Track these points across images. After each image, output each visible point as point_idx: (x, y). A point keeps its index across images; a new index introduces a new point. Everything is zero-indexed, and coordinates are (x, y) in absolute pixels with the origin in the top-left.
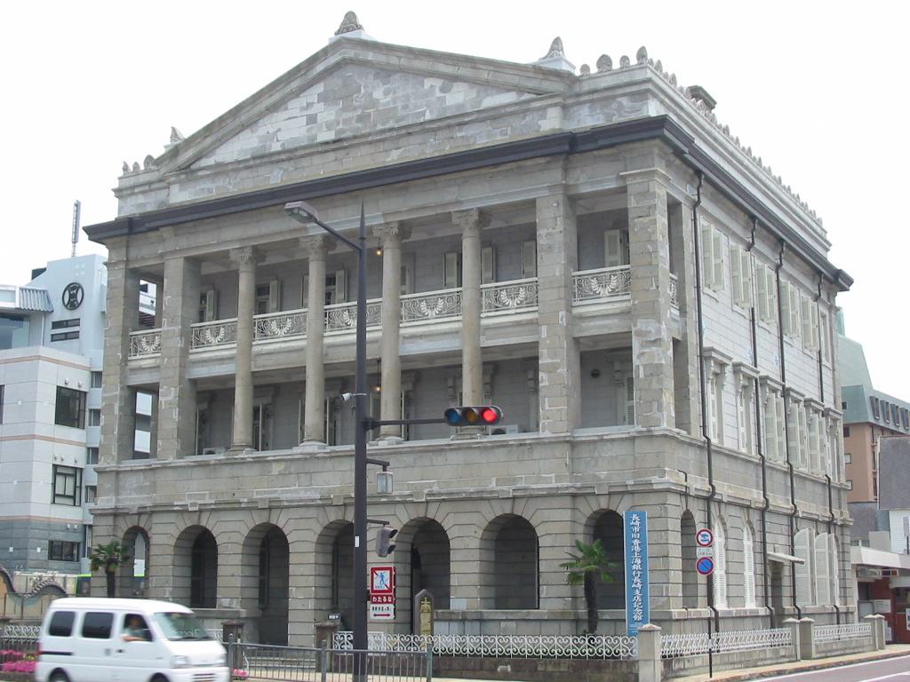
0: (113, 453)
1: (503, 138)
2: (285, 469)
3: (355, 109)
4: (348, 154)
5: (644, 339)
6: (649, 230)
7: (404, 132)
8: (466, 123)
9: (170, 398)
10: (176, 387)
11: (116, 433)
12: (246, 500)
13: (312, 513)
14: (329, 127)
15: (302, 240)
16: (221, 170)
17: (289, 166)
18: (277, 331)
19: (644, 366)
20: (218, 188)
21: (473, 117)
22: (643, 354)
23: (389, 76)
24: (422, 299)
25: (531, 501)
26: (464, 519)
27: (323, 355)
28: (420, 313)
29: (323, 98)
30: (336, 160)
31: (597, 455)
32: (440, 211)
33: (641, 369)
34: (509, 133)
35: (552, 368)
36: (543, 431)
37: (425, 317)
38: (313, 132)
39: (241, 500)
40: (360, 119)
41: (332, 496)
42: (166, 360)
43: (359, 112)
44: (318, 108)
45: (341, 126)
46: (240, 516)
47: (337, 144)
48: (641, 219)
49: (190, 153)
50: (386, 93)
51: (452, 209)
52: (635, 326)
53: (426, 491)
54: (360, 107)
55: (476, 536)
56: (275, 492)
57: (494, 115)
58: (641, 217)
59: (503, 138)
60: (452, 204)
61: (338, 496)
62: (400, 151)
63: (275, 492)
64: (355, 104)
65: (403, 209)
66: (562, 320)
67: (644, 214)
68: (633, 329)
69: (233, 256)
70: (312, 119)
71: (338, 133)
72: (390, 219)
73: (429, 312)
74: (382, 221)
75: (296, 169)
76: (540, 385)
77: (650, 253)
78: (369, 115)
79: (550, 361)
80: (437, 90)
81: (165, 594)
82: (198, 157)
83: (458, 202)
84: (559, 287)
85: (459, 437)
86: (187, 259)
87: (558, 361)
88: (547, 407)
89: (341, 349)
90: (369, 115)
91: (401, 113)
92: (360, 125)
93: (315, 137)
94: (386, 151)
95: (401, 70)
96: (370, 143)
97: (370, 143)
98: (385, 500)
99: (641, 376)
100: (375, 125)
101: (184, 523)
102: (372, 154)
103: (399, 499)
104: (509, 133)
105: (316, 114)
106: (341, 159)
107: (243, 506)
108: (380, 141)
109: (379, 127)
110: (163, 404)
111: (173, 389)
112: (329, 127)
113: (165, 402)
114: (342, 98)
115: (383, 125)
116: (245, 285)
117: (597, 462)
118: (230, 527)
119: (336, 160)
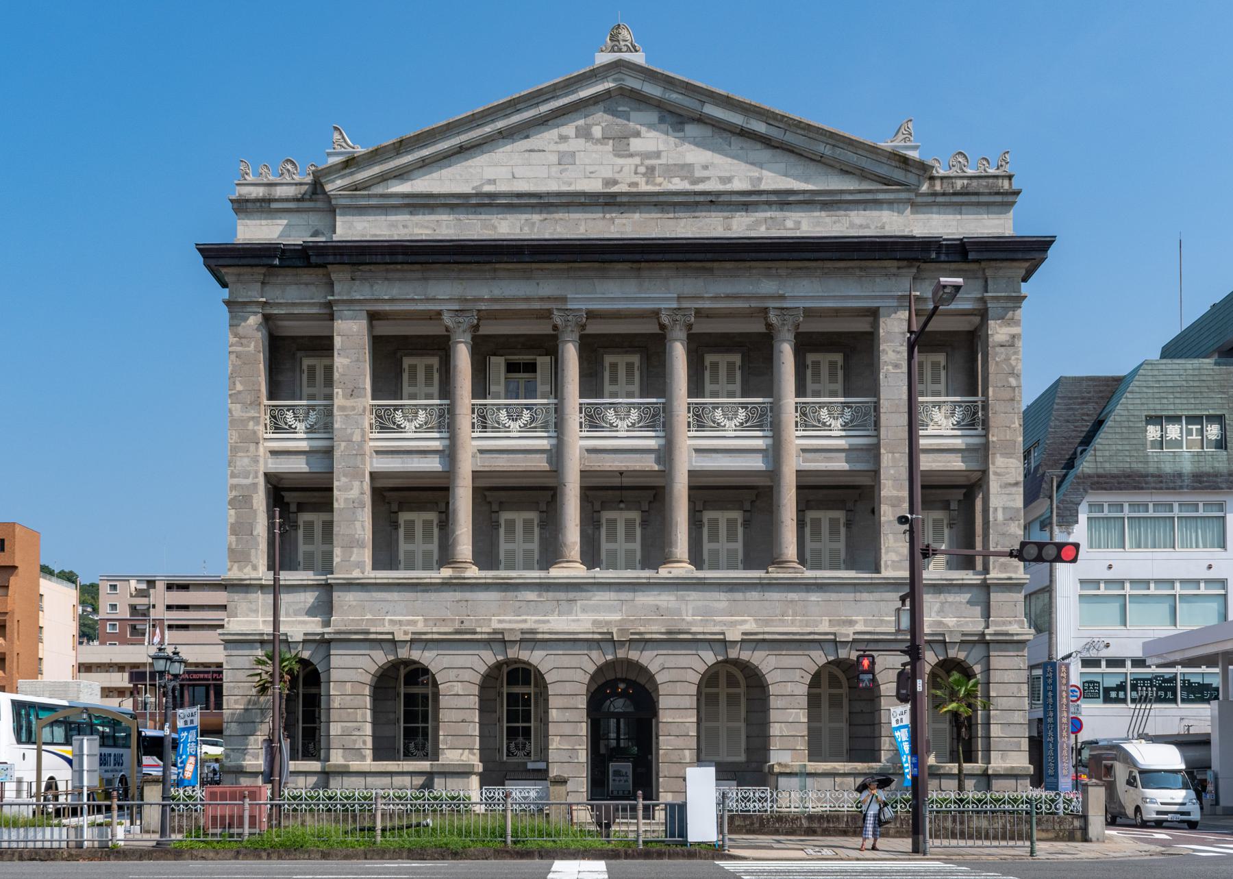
3: (631, 155)
8: (789, 203)
9: (354, 493)
19: (1004, 509)
21: (800, 198)
23: (682, 123)
51: (771, 304)
52: (993, 464)
55: (802, 680)
56: (525, 621)
60: (772, 297)
63: (525, 621)
65: (706, 295)
72: (685, 305)
74: (675, 306)
76: (882, 518)
77: (1014, 388)
82: (384, 178)
83: (782, 297)
91: (699, 173)
95: (701, 120)
101: (381, 658)
111: (356, 484)
114: (614, 139)
116: (463, 357)
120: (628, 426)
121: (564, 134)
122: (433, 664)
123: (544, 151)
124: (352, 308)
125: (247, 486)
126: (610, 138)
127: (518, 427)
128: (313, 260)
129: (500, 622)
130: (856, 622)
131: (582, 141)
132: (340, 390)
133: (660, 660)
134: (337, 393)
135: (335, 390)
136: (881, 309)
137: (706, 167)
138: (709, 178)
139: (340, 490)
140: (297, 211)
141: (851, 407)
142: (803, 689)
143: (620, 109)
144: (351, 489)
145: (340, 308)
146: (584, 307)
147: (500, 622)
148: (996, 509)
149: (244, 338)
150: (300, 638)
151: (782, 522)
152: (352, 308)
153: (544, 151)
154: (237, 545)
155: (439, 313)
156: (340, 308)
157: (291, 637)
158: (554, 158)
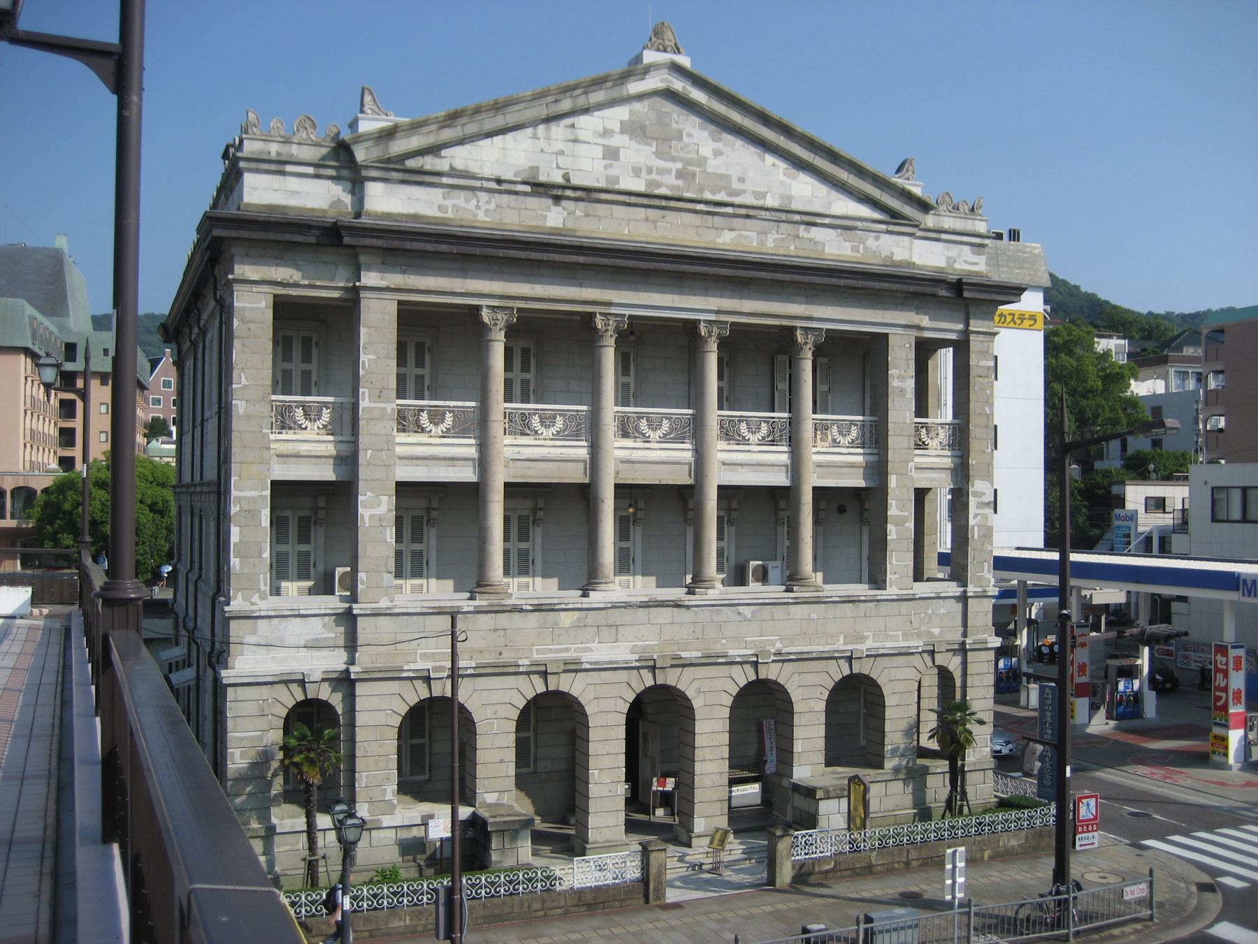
0: (262, 587)
1: (855, 254)
2: (579, 620)
3: (674, 160)
4: (664, 217)
5: (979, 500)
6: (988, 392)
7: (743, 211)
10: (390, 496)
11: (267, 554)
12: (527, 662)
13: (621, 676)
14: (637, 172)
15: (598, 316)
16: (464, 181)
17: (579, 209)
18: (541, 430)
20: (456, 208)
21: (827, 221)
22: (976, 515)
24: (741, 418)
25: (878, 658)
26: (809, 679)
27: (617, 473)
28: (739, 435)
29: (627, 128)
30: (647, 219)
31: (930, 611)
32: (785, 323)
33: (976, 528)
34: (861, 250)
35: (900, 522)
36: (890, 587)
37: (745, 441)
38: (612, 172)
39: (520, 662)
40: (680, 175)
41: (655, 657)
42: (369, 452)
43: (679, 165)
44: (619, 140)
45: (654, 176)
46: (510, 681)
47: (649, 200)
48: (980, 379)
49: (415, 142)
50: (717, 153)
52: (973, 486)
53: (773, 651)
54: (681, 159)
56: (567, 650)
57: (845, 225)
58: (980, 376)
59: (855, 254)
61: (664, 656)
62: (734, 234)
63: (567, 650)
64: (674, 154)
66: (911, 472)
67: (984, 375)
68: (970, 490)
69: (486, 316)
70: (611, 154)
71: (650, 183)
72: (723, 318)
73: (749, 436)
74: (713, 317)
75: (587, 215)
76: (888, 537)
78: (694, 175)
79: (900, 513)
80: (781, 171)
81: (385, 795)
84: (909, 436)
85: (803, 589)
86: (400, 303)
87: (906, 514)
88: (894, 562)
89: (637, 466)
90: (694, 175)
91: (735, 185)
92: (680, 183)
93: (616, 180)
94: (717, 229)
96: (696, 212)
97: (696, 212)
98: (724, 660)
99: (976, 537)
100: (701, 190)
102: (697, 227)
103: (740, 660)
104: (861, 250)
105: (619, 148)
106: (654, 221)
107: (521, 669)
108: (709, 213)
109: (708, 196)
110: (367, 519)
112: (637, 172)
113: (371, 517)
114: (657, 140)
115: (713, 193)
117: (930, 618)
118: (497, 697)
119: (647, 219)
120: (659, 437)
121: (610, 127)
122: (469, 701)
123: (589, 143)
124: (382, 296)
125: (254, 499)
126: (653, 138)
127: (551, 435)
128: (347, 240)
129: (539, 652)
130: (867, 637)
131: (626, 137)
132: (366, 390)
133: (696, 684)
134: (364, 393)
135: (361, 390)
136: (890, 336)
137: (742, 180)
138: (744, 192)
139: (366, 507)
140: (317, 176)
141: (857, 425)
142: (822, 706)
143: (664, 110)
144: (379, 505)
145: (368, 295)
146: (627, 313)
147: (539, 652)
148: (973, 527)
149: (251, 322)
150: (317, 676)
151: (803, 540)
152: (382, 296)
153: (589, 143)
154: (241, 568)
155: (477, 308)
156: (368, 295)
157: (309, 675)
158: (599, 151)
